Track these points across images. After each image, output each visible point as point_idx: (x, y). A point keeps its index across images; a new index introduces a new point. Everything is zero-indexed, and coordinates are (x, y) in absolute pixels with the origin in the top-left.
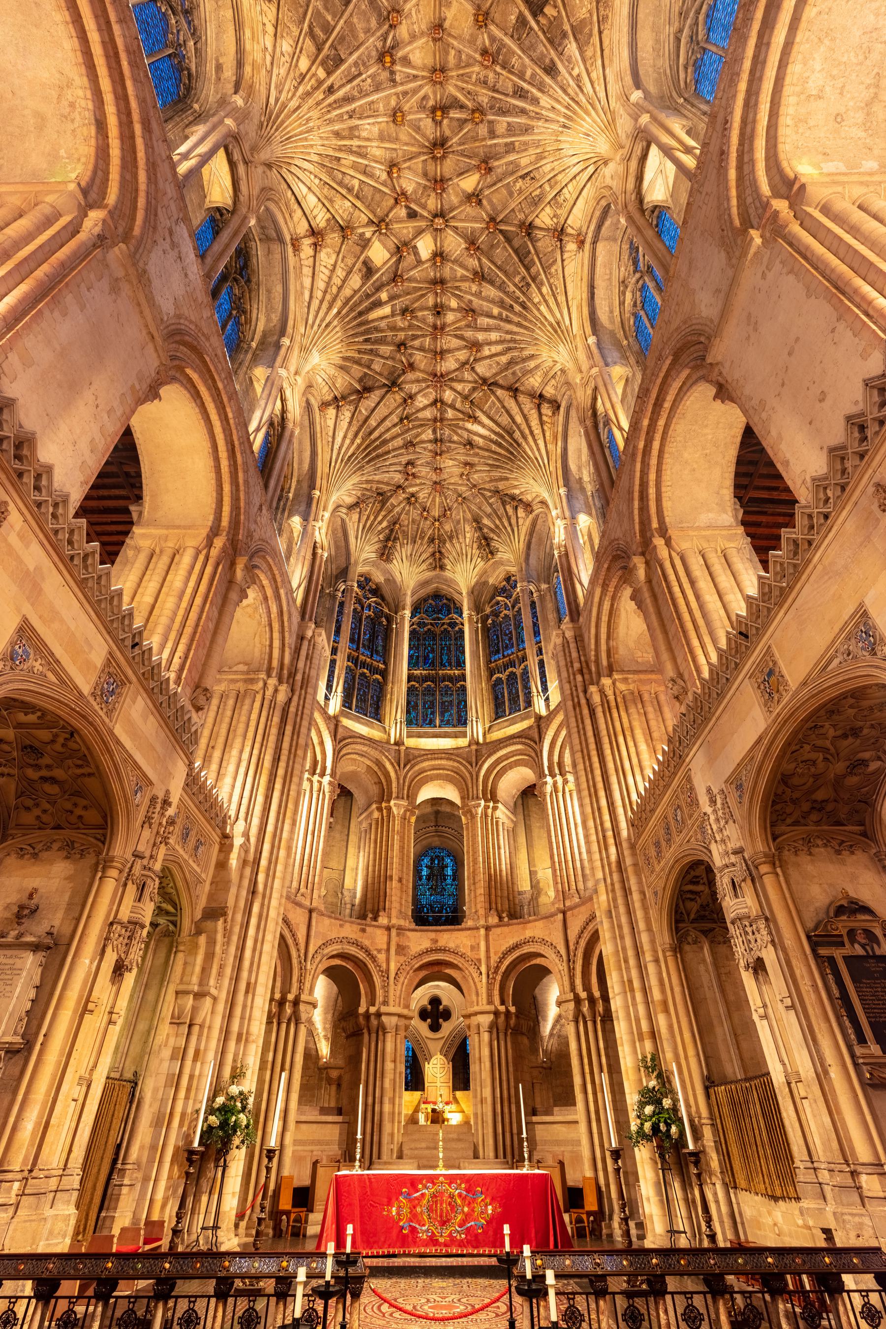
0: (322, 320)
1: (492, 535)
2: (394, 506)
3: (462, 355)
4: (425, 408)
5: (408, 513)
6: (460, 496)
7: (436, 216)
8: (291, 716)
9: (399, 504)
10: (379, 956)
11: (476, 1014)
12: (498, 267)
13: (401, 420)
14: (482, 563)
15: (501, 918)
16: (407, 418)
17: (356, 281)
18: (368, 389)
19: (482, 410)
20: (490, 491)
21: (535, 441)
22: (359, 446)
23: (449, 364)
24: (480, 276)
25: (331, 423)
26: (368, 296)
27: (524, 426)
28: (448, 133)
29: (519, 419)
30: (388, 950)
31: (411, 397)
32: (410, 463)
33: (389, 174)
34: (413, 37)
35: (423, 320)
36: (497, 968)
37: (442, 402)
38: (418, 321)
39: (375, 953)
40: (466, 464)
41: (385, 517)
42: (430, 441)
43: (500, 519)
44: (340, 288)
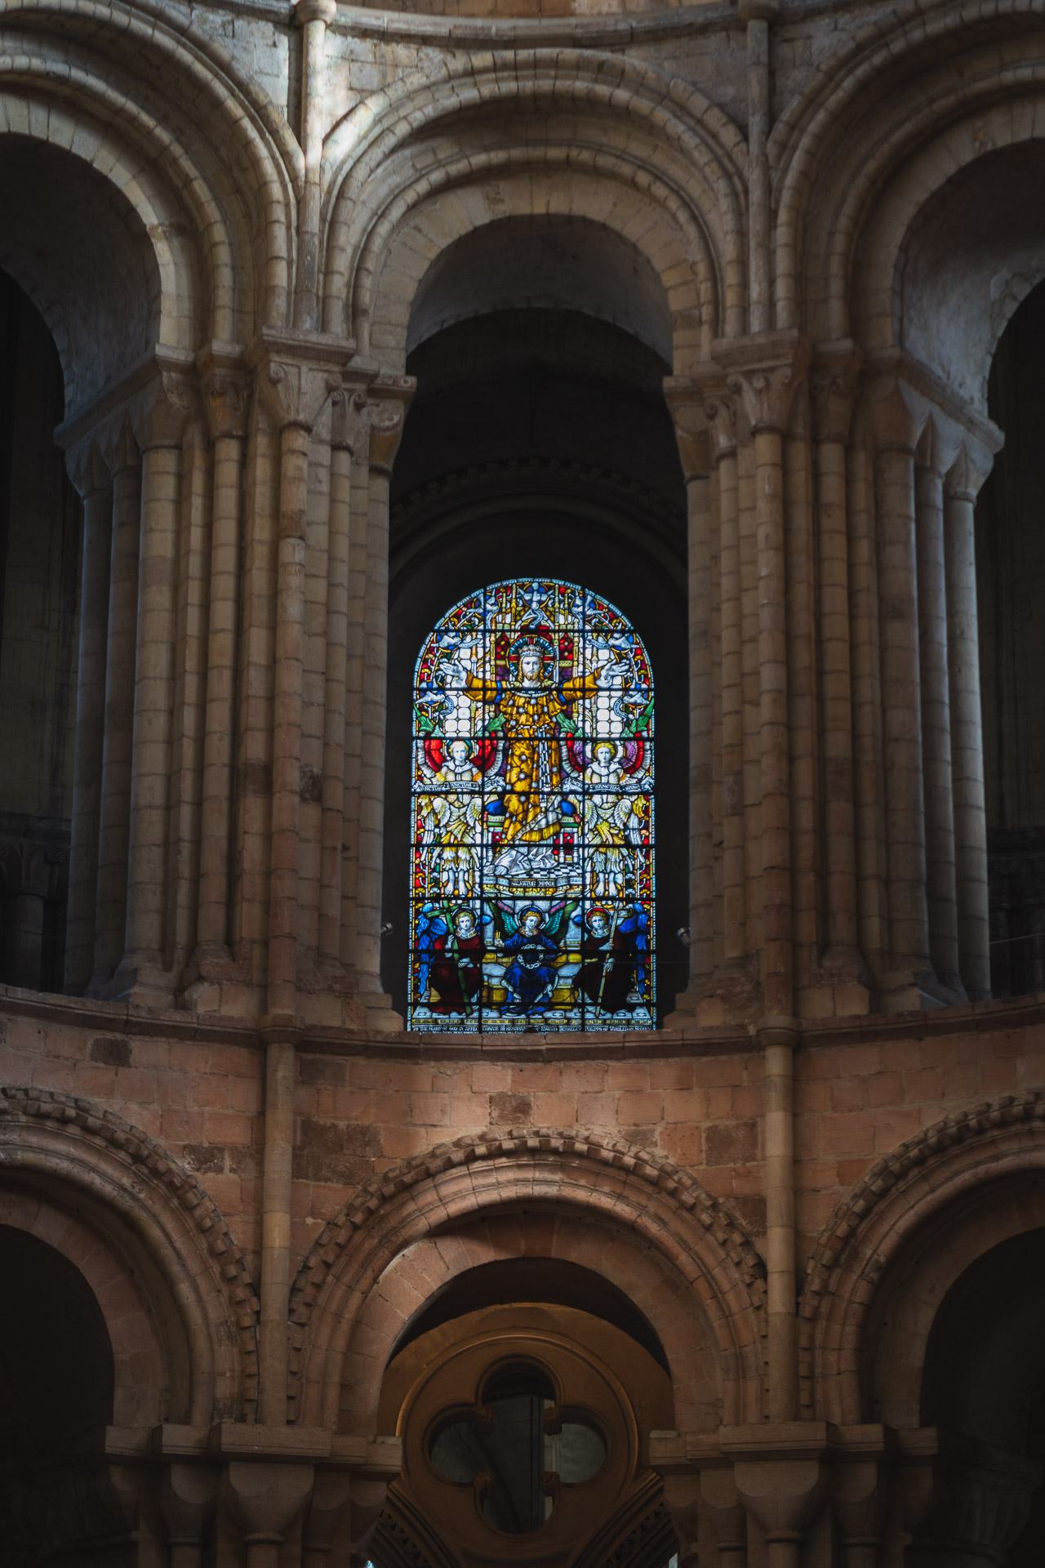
10: (207, 1181)
11: (726, 1460)
30: (258, 1151)
36: (847, 1248)
39: (184, 1165)
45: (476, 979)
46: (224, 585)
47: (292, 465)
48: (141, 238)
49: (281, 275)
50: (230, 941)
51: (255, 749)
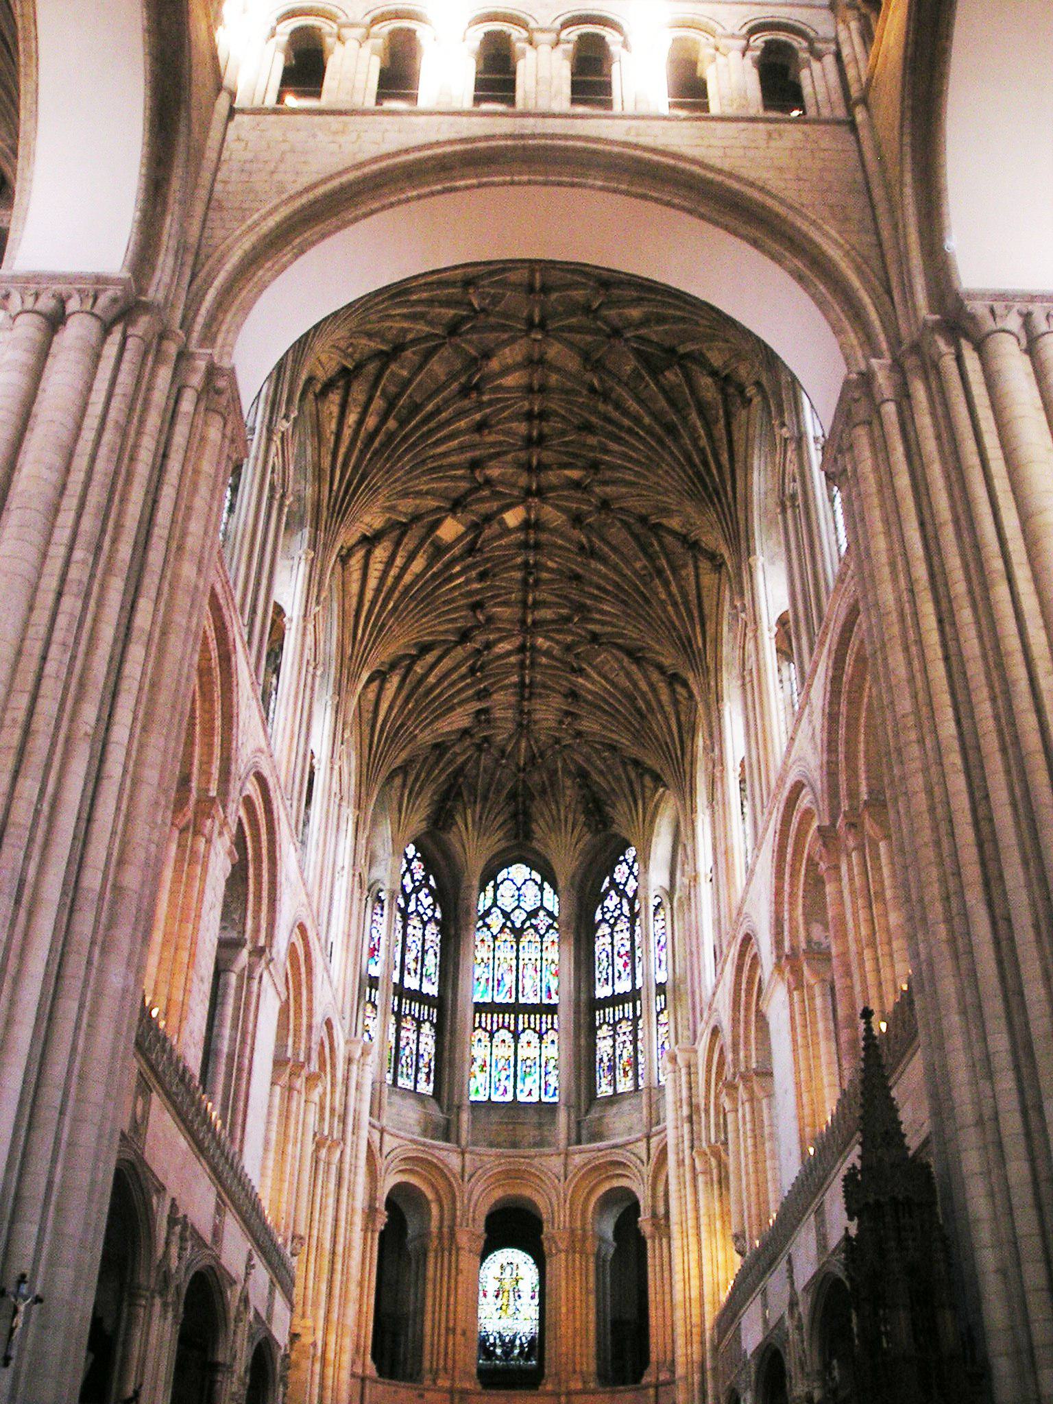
0: (374, 625)
1: (604, 797)
2: (456, 755)
3: (564, 611)
4: (508, 654)
5: (478, 762)
6: (557, 741)
7: (528, 492)
8: (346, 1175)
9: (464, 752)
12: (614, 549)
13: (472, 671)
14: (588, 837)
15: (584, 1382)
16: (482, 668)
17: (418, 565)
18: (425, 649)
19: (590, 664)
20: (603, 744)
21: (667, 719)
22: (411, 712)
23: (546, 614)
24: (589, 552)
25: (371, 696)
26: (434, 577)
27: (650, 696)
28: (546, 430)
29: (644, 686)
31: (488, 646)
32: (485, 711)
33: (472, 472)
34: (506, 371)
35: (512, 579)
37: (534, 648)
38: (502, 579)
40: (568, 713)
41: (442, 771)
42: (514, 685)
43: (618, 779)
44: (399, 578)
45: (494, 1352)
46: (445, 1285)
47: (461, 1258)
48: (428, 1203)
49: (458, 1213)
50: (445, 1369)
51: (451, 1325)
